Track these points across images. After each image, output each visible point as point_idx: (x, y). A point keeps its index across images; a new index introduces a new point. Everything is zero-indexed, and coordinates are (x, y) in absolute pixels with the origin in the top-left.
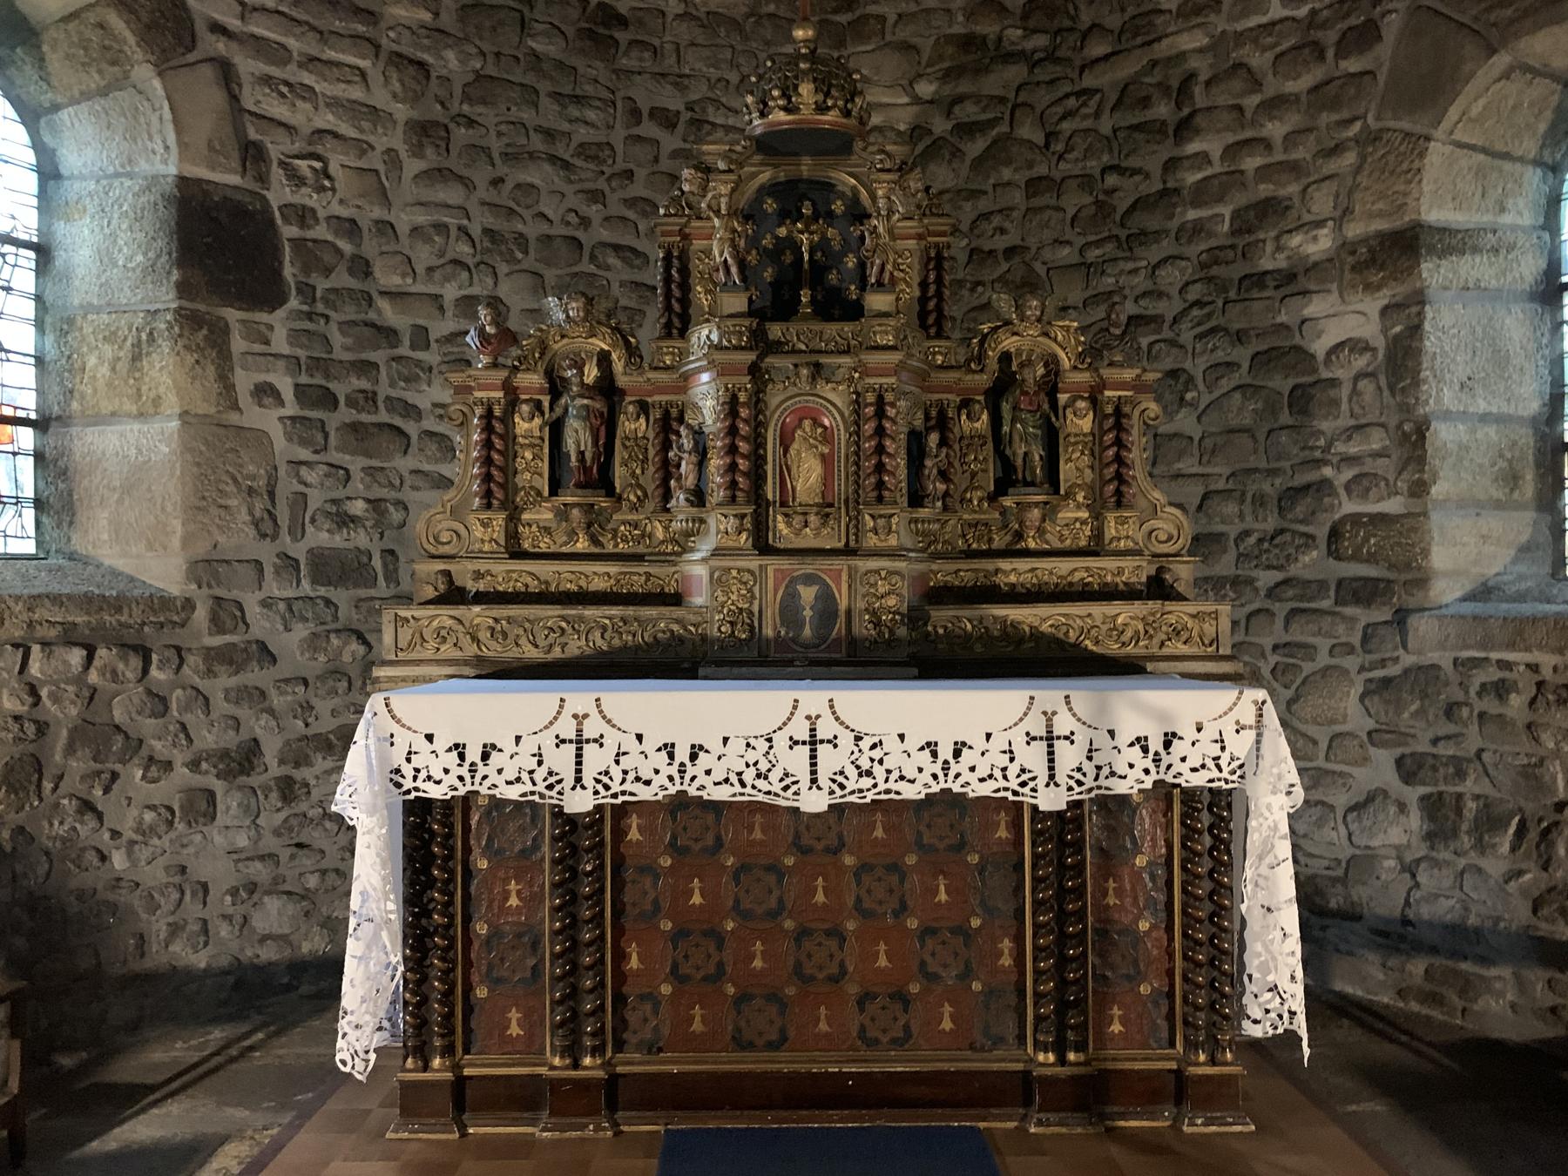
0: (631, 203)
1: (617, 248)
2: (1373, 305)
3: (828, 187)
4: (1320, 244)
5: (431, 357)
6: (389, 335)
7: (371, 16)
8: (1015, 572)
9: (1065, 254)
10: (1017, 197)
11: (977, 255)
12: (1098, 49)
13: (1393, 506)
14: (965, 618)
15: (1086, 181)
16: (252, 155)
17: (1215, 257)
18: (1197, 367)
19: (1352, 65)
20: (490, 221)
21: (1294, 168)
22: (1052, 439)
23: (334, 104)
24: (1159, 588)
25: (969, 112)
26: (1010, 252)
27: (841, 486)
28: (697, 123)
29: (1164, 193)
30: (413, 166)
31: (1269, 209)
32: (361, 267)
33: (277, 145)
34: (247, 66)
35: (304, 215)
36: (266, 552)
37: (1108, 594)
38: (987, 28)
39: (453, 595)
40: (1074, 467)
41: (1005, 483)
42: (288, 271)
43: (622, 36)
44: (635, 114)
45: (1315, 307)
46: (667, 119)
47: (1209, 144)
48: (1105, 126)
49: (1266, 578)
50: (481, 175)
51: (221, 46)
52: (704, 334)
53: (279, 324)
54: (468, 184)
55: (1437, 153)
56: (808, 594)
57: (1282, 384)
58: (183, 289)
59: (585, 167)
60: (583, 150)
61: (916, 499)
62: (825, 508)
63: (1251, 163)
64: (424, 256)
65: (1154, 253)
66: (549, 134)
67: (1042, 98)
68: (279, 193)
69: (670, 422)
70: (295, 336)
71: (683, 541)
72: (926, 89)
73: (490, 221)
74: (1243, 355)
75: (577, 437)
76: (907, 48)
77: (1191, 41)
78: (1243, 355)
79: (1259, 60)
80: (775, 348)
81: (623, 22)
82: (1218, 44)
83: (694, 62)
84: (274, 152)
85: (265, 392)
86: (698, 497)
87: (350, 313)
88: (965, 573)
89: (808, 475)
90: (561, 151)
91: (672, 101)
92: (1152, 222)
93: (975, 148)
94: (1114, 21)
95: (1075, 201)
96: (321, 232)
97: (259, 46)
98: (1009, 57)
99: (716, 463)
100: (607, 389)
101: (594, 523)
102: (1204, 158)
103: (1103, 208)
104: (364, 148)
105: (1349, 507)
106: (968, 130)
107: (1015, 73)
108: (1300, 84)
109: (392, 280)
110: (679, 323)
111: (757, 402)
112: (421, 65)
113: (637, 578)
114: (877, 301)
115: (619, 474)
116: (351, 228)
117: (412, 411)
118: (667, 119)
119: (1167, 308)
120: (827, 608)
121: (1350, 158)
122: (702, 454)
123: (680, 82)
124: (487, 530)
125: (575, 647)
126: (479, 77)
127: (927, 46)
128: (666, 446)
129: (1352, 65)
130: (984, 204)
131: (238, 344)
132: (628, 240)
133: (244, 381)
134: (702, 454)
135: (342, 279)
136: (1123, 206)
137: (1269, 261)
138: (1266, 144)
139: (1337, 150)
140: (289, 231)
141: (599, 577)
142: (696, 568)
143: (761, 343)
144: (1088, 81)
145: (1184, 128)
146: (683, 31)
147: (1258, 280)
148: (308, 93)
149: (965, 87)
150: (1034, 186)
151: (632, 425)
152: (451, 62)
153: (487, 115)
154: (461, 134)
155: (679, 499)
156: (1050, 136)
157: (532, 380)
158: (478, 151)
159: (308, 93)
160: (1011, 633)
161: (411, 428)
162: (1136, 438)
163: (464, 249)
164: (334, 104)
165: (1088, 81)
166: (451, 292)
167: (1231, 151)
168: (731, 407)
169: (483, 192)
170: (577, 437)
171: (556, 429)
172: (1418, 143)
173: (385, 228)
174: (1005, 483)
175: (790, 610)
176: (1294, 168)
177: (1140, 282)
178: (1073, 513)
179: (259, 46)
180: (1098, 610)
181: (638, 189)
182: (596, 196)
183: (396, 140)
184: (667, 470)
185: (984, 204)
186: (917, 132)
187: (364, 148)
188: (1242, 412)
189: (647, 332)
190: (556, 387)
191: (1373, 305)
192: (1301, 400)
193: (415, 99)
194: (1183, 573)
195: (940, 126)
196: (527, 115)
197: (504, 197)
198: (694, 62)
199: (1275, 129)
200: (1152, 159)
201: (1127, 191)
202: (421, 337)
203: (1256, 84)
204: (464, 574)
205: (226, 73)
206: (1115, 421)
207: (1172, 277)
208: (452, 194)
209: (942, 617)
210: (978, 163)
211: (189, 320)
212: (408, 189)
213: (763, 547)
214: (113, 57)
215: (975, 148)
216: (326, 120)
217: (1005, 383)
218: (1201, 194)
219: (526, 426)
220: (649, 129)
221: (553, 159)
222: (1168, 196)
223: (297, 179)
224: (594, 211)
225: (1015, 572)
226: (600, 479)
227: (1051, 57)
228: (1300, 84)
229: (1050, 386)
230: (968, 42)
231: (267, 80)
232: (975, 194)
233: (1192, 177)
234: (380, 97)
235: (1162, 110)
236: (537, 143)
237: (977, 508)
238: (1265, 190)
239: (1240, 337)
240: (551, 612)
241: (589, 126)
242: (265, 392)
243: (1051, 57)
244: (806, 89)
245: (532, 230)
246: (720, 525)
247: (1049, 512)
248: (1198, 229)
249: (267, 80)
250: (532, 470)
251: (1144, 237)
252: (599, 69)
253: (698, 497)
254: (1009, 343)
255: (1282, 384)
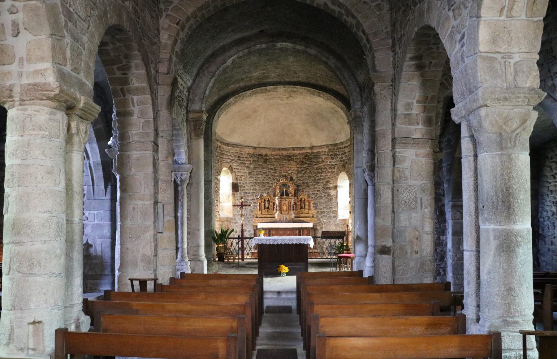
0: (269, 178)
1: (267, 183)
2: (335, 191)
3: (286, 185)
4: (331, 185)
5: (250, 195)
6: (246, 193)
7: (245, 163)
8: (301, 215)
9: (311, 184)
10: (307, 177)
11: (304, 183)
12: (314, 164)
13: (336, 209)
14: (297, 219)
15: (313, 177)
16: (237, 178)
17: (324, 185)
18: (323, 195)
19: (334, 170)
20: (255, 181)
21: (330, 178)
22: (305, 205)
23: (242, 173)
24: (313, 217)
25: (302, 169)
26: (306, 183)
27: (287, 209)
28: (275, 170)
29: (320, 179)
30: (249, 177)
31: (328, 182)
32: (244, 187)
33: (238, 177)
34: (236, 171)
35: (240, 183)
36: (238, 214)
37: (309, 217)
38: (304, 160)
39: (257, 217)
40: (307, 207)
41: (301, 208)
42: (239, 188)
43: (268, 161)
44: (269, 169)
45: (331, 191)
46: (271, 169)
47: (324, 175)
48: (315, 171)
49: (328, 216)
50: (254, 177)
51: (234, 170)
52: (277, 198)
53: (238, 193)
54: (253, 178)
55: (339, 179)
56: (285, 217)
57: (329, 198)
58: (233, 191)
59: (264, 175)
60: (264, 173)
61: (293, 210)
62: (286, 210)
63: (327, 177)
64: (249, 185)
65: (319, 184)
66: (261, 172)
67: (309, 168)
68: (239, 182)
69: (274, 204)
70: (240, 194)
71: (275, 213)
72: (298, 166)
73: (255, 181)
74: (326, 195)
75: (267, 205)
76: (296, 162)
77: (322, 165)
78: (326, 195)
79: (327, 168)
80: (282, 198)
81: (267, 160)
82: (324, 165)
83: (275, 163)
84: (238, 178)
85: (237, 199)
86: (276, 210)
87: (243, 191)
88: (298, 215)
89: (285, 208)
90: (262, 173)
91: (272, 167)
92: (319, 181)
93: (303, 172)
94: (316, 161)
95: (312, 178)
96: (241, 184)
97: (237, 169)
98: (306, 163)
99: (278, 207)
100: (269, 201)
101: (268, 211)
102: (323, 176)
103: (315, 179)
104: (244, 176)
105: (334, 209)
106: (302, 170)
107: (307, 165)
108: (330, 171)
109: (247, 188)
110: (275, 196)
111: (281, 203)
112: (249, 167)
113: (271, 216)
114: (290, 195)
115: (270, 208)
116: (243, 183)
117: (248, 200)
118: (271, 169)
119: (321, 190)
120: (286, 219)
121: (333, 179)
122: (277, 206)
123: (273, 165)
124: (259, 212)
125: (267, 221)
126: (254, 167)
127: (298, 161)
128: (274, 206)
129: (334, 170)
130: (304, 178)
131: (236, 195)
132: (268, 182)
133: (236, 199)
134: (277, 206)
135: (243, 188)
136: (317, 179)
137: (328, 186)
138: (328, 175)
139: (332, 177)
140: (239, 185)
141: (269, 216)
142: (276, 215)
143: (282, 198)
144: (314, 167)
145: (322, 173)
146: (274, 160)
147: (327, 188)
148: (240, 172)
149: (302, 166)
150: (309, 176)
151: (271, 204)
152: (252, 166)
153: (255, 171)
154: (253, 173)
155: (275, 210)
156: (310, 172)
157: (263, 200)
158: (254, 174)
159: (240, 172)
160: (300, 220)
161: (248, 202)
162: (311, 204)
163: (253, 184)
164: (242, 173)
165: (314, 167)
166: (252, 188)
167: (326, 175)
168: (279, 203)
169: (255, 178)
170: (267, 205)
171: (265, 204)
172: (337, 178)
173: (246, 183)
174: (301, 208)
175: (283, 219)
176: (330, 178)
177: (318, 187)
178: (306, 211)
179: (237, 169)
180: (306, 218)
181: (269, 176)
182: (265, 178)
183: (247, 174)
184: (274, 208)
185: (304, 178)
186: (297, 170)
187: (244, 176)
188: (326, 200)
189: (272, 196)
190: (265, 201)
191: (335, 191)
192: (331, 199)
193: (248, 170)
194: (315, 216)
195: (300, 170)
196: (259, 170)
197: (256, 179)
198: (275, 163)
199: (329, 174)
200: (319, 175)
201: (317, 178)
202: (249, 193)
203: (327, 170)
204: (258, 216)
205: (235, 171)
206: (310, 203)
207: (321, 187)
208: (252, 179)
209: (295, 219)
210: (303, 174)
211: (233, 194)
212: (248, 179)
213: (281, 214)
214: (228, 173)
215: (303, 172)
216: (242, 174)
217: (301, 200)
218: (323, 179)
219: (263, 204)
220: (270, 170)
221: (261, 174)
222: (320, 179)
223: (240, 180)
224: (265, 179)
225: (301, 215)
226: (268, 208)
227: (310, 164)
228: (330, 171)
229: (305, 200)
230: (302, 161)
231: (238, 172)
232: (303, 177)
233: (322, 178)
234: (246, 171)
235: (320, 171)
236: (259, 173)
237: (299, 210)
238: (328, 180)
239: (326, 193)
240: (265, 219)
241: (265, 170)
242: (237, 199)
243: (310, 164)
244: (284, 180)
245: (259, 181)
246: (278, 212)
247: (304, 211)
248: (323, 183)
249: (238, 172)
250: (263, 207)
251: (318, 183)
252: (265, 165)
253: (276, 210)
254: (301, 197)
255: (329, 198)
